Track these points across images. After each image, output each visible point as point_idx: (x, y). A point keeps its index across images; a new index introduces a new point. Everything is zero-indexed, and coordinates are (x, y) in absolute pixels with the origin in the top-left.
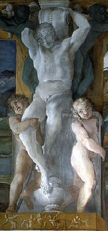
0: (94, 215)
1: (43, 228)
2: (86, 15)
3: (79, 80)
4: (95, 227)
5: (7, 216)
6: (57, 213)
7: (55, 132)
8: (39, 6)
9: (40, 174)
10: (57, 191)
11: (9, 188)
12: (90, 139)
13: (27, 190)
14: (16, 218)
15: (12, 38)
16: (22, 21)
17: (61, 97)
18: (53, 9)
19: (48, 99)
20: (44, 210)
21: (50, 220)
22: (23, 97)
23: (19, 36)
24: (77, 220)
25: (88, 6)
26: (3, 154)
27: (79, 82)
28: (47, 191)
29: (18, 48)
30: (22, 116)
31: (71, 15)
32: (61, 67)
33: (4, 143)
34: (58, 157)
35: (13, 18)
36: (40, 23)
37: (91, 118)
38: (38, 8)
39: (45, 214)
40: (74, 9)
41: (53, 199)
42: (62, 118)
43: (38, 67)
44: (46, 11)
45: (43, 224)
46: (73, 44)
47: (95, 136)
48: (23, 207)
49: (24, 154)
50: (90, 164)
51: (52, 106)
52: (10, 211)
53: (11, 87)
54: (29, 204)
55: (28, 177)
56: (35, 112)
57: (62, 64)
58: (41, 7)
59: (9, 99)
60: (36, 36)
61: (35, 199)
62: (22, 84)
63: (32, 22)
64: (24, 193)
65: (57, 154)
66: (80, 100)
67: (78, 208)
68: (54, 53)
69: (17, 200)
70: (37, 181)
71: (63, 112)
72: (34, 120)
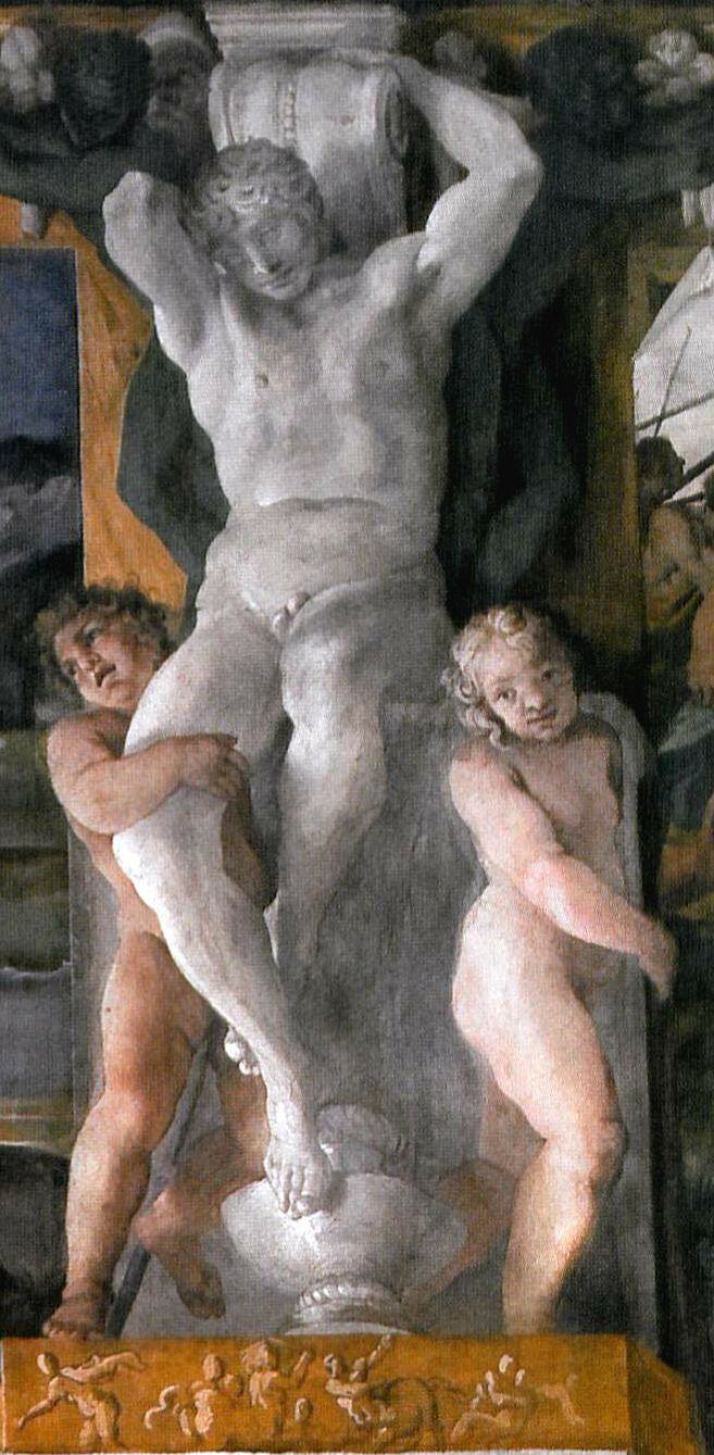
0: (615, 1353)
1: (285, 1437)
2: (509, 101)
3: (479, 497)
4: (623, 1428)
5: (53, 1361)
6: (380, 1337)
7: (346, 824)
8: (212, 41)
9: (256, 1088)
10: (366, 1194)
11: (58, 1171)
12: (568, 859)
13: (176, 1192)
14: (111, 1374)
15: (43, 231)
16: (104, 133)
17: (383, 597)
18: (295, 58)
19: (288, 616)
20: (290, 1322)
21: (333, 1386)
22: (133, 602)
23: (89, 222)
24: (505, 1384)
25: (521, 45)
26: (13, 962)
27: (483, 507)
28: (310, 1200)
29: (85, 298)
30: (124, 718)
31: (420, 100)
32: (366, 416)
33: (20, 891)
34: (369, 984)
35: (45, 115)
36: (222, 142)
37: (571, 732)
38: (207, 55)
39: (297, 1346)
40: (430, 63)
41: (351, 1253)
42: (387, 737)
43: (219, 413)
44: (252, 72)
45: (287, 1411)
46: (435, 272)
47: (602, 842)
48: (154, 1301)
49: (148, 962)
50: (570, 1019)
51: (317, 658)
52: (71, 1328)
53: (48, 538)
54: (194, 1280)
55: (183, 1107)
56: (216, 694)
57: (367, 393)
58: (226, 49)
59: (46, 618)
60: (199, 224)
61: (227, 1248)
62: (117, 524)
63: (166, 141)
64: (161, 1214)
65: (360, 956)
66: (499, 620)
67: (511, 1306)
68: (322, 322)
69: (111, 1268)
70: (240, 1136)
71: (390, 694)
72: (209, 751)
